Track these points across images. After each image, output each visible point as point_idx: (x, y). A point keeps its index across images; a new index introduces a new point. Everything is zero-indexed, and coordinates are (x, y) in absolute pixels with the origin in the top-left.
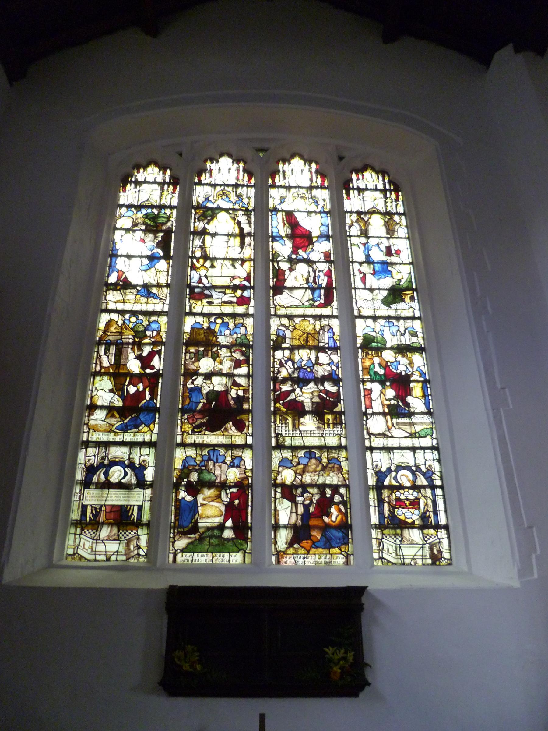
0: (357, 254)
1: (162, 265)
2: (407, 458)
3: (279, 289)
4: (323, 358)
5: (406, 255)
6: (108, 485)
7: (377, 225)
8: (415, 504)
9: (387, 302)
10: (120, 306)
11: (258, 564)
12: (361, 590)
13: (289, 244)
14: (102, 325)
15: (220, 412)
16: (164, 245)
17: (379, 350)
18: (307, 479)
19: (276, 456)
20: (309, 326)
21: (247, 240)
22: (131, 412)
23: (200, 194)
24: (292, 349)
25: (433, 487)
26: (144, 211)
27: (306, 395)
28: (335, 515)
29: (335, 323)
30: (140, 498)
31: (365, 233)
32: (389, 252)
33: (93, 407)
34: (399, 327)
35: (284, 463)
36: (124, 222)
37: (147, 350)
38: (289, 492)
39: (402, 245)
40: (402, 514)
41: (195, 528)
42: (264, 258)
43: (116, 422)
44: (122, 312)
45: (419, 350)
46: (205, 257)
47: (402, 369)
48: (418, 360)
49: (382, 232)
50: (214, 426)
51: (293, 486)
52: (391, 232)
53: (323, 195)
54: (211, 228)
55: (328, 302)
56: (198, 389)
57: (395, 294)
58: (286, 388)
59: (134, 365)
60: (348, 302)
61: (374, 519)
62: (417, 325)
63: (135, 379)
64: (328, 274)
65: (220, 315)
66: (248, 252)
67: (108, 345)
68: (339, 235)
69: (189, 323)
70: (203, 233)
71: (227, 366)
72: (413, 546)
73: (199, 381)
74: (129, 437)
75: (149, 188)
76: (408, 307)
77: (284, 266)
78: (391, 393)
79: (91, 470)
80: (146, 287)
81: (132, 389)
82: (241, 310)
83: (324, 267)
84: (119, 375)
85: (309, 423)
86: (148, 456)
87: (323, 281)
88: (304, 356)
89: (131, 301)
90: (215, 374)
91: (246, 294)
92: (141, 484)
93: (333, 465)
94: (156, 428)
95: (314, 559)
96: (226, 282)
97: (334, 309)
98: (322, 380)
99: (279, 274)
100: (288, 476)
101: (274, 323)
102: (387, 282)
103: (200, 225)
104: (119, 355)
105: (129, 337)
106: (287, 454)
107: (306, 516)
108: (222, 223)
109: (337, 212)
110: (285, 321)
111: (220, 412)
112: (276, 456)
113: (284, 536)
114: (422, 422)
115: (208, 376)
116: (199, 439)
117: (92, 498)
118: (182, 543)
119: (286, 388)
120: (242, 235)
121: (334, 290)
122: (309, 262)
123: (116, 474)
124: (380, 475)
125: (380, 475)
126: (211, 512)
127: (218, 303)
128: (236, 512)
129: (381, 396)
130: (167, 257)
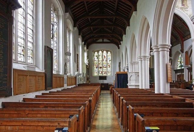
7: (109, 56)
11: (103, 75)
15: (101, 68)
23: (99, 54)
27: (105, 67)
34: (109, 63)
39: (110, 57)
42: (103, 59)
53: (106, 54)
57: (110, 61)
72: (109, 74)
75: (96, 54)
76: (110, 61)
84: (96, 66)
86: (97, 70)
90: (101, 66)
108: (100, 56)
111: (101, 68)
121: (107, 61)
126: (100, 72)
129: (109, 67)
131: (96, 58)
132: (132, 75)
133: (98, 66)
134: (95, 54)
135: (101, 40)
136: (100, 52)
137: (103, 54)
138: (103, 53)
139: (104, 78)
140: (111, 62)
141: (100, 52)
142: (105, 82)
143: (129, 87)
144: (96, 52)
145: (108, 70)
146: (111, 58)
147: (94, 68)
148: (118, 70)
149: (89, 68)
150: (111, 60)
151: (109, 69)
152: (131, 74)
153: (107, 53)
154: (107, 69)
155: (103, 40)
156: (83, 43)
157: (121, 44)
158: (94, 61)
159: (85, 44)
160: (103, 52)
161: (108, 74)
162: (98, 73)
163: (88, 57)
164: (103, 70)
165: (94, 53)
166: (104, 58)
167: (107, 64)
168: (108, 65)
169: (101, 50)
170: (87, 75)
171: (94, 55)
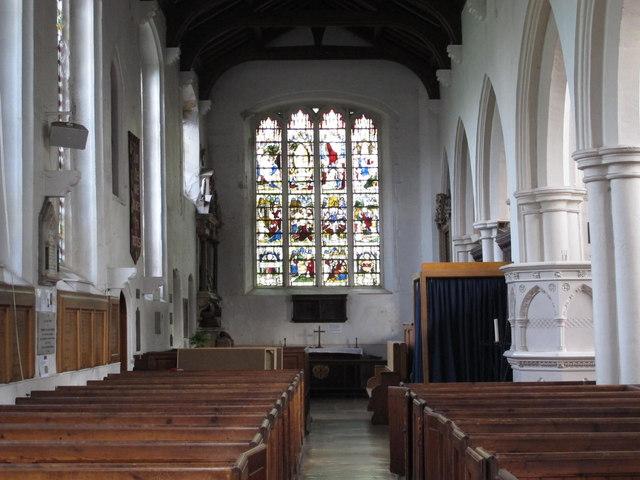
0: (355, 164)
1: (278, 172)
2: (368, 249)
3: (324, 182)
4: (341, 211)
5: (376, 164)
6: (267, 261)
7: (365, 146)
8: (369, 265)
9: (366, 187)
10: (263, 192)
12: (346, 295)
13: (328, 159)
14: (258, 200)
15: (304, 234)
16: (277, 162)
17: (361, 207)
18: (334, 257)
19: (324, 249)
20: (336, 198)
21: (312, 158)
22: (272, 234)
23: (290, 134)
24: (329, 208)
25: (376, 260)
26: (268, 145)
27: (334, 227)
28: (342, 270)
29: (345, 196)
30: (278, 265)
31: (359, 153)
32: (369, 163)
33: (259, 233)
35: (326, 252)
36: (260, 152)
37: (276, 210)
38: (327, 262)
39: (374, 158)
40: (365, 269)
41: (297, 275)
42: (317, 167)
43: (268, 238)
44: (264, 194)
45: (376, 207)
46: (295, 168)
47: (369, 216)
48: (376, 212)
49: (367, 151)
50: (302, 239)
51: (329, 260)
52: (370, 153)
53: (343, 133)
54: (296, 153)
55: (343, 188)
56: (295, 225)
57: (370, 183)
58: (327, 224)
59: (272, 217)
60: (350, 187)
61: (356, 270)
62: (377, 197)
63: (273, 222)
64: (343, 174)
65: (302, 194)
66: (312, 164)
67: (261, 208)
68: (349, 155)
69: (290, 197)
70: (293, 155)
71: (305, 216)
73: (296, 222)
74: (273, 244)
75: (268, 132)
76: (375, 188)
77: (326, 170)
78: (364, 225)
79: (261, 256)
80: (272, 182)
81: (272, 226)
82: (309, 192)
83: (342, 170)
84: (266, 220)
85: (335, 236)
86: (280, 251)
87: (341, 177)
88: (333, 211)
89: (267, 189)
90: (302, 219)
91: (312, 184)
92: (279, 260)
93: (343, 252)
94: (281, 240)
95: (337, 283)
96: (303, 179)
97: (345, 191)
98: (340, 220)
99: (324, 174)
100: (327, 257)
101: (322, 197)
102: (367, 177)
103: (290, 152)
104: (265, 211)
105: (268, 205)
106: (327, 248)
107: (333, 270)
108: (300, 150)
109: (348, 142)
110: (326, 196)
111: (304, 234)
112: (324, 249)
113: (326, 276)
114: (375, 236)
115: (299, 220)
116: (296, 244)
117: (263, 265)
118: (293, 279)
119: (327, 224)
120: (309, 156)
121: (346, 182)
122: (335, 168)
123: (270, 257)
124: (358, 256)
125: (358, 256)
126: (302, 269)
127: (301, 188)
128: (310, 269)
129: (361, 226)
130: (279, 168)
131: (265, 162)
132: (536, 290)
133: (287, 219)
134: (260, 137)
135: (302, 37)
136: (300, 120)
137: (316, 135)
138: (316, 131)
139: (327, 308)
140: (381, 193)
141: (300, 120)
142: (334, 338)
143: (521, 375)
144: (268, 124)
145: (357, 251)
146: (380, 168)
147: (255, 234)
148: (427, 259)
149: (218, 235)
150: (381, 178)
151: (367, 245)
152: (527, 281)
153: (350, 128)
154: (351, 246)
155: (318, 34)
156: (175, 54)
157: (447, 64)
158: (255, 183)
159: (183, 65)
160: (316, 121)
161: (359, 280)
162: (285, 274)
163: (208, 157)
164: (319, 247)
165: (256, 127)
166: (325, 162)
167: (352, 206)
168: (357, 213)
169: (307, 110)
170: (201, 288)
171: (253, 142)
